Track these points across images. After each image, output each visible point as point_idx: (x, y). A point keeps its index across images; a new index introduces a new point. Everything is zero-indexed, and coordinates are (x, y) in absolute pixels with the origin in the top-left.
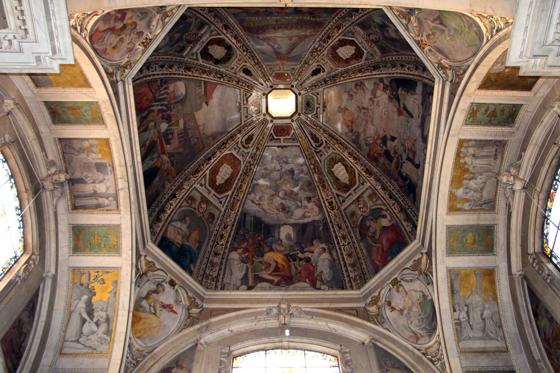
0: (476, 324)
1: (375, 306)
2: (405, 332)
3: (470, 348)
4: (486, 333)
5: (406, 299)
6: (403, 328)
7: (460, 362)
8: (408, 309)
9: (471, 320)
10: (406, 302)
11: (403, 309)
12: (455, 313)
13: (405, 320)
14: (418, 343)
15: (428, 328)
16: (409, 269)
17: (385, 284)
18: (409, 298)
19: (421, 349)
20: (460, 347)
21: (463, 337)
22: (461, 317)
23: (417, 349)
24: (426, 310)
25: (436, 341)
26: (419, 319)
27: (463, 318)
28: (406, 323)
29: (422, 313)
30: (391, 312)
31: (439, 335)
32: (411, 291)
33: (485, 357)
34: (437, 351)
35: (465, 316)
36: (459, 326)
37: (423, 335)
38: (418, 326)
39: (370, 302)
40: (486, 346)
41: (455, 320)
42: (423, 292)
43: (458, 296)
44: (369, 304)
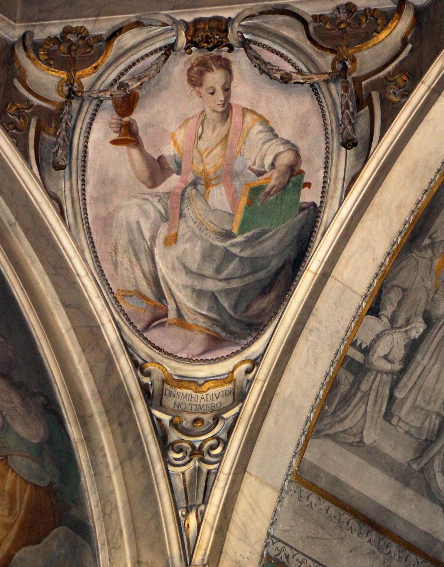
0: (414, 407)
1: (63, 75)
2: (123, 259)
3: (336, 481)
4: (425, 460)
5: (208, 132)
6: (123, 240)
7: (275, 511)
8: (191, 178)
9: (408, 381)
10: (202, 145)
11: (173, 166)
12: (371, 320)
13: (153, 214)
14: (150, 335)
15: (226, 304)
16: (305, 23)
17: (162, 15)
18: (227, 136)
19: (151, 367)
20: (307, 455)
21: (339, 428)
22: (382, 349)
23: (131, 356)
24: (263, 233)
25: (229, 378)
26: (213, 247)
27: (386, 357)
28: (146, 227)
29: (242, 231)
30: (114, 142)
31: (256, 363)
32: (249, 118)
33: (368, 547)
34: (207, 418)
35: (399, 353)
36: (351, 378)
37: (189, 319)
38: (188, 271)
39: (49, 39)
40: (392, 508)
41: (353, 344)
42: (297, 155)
43: (423, 264)
44: (37, 46)
